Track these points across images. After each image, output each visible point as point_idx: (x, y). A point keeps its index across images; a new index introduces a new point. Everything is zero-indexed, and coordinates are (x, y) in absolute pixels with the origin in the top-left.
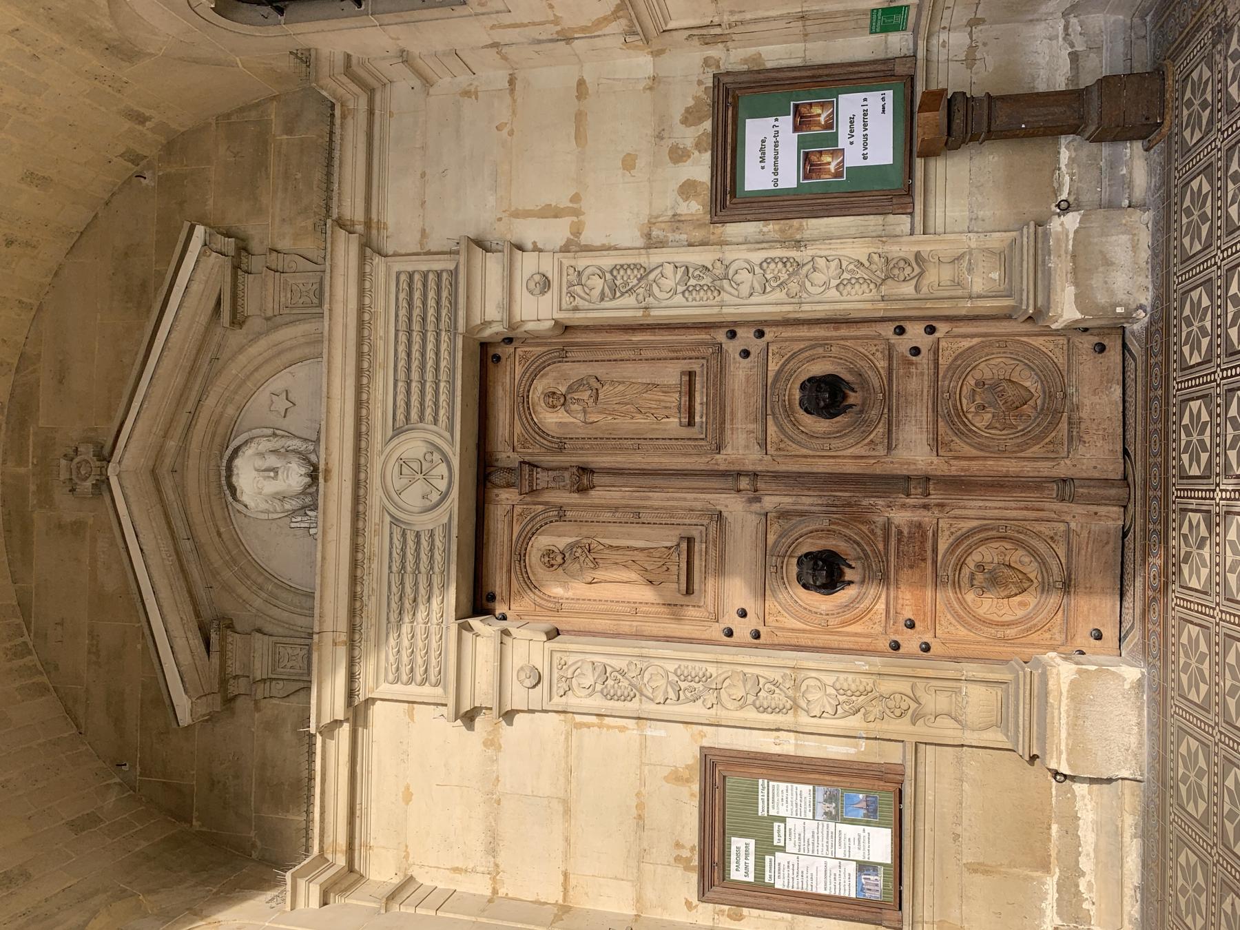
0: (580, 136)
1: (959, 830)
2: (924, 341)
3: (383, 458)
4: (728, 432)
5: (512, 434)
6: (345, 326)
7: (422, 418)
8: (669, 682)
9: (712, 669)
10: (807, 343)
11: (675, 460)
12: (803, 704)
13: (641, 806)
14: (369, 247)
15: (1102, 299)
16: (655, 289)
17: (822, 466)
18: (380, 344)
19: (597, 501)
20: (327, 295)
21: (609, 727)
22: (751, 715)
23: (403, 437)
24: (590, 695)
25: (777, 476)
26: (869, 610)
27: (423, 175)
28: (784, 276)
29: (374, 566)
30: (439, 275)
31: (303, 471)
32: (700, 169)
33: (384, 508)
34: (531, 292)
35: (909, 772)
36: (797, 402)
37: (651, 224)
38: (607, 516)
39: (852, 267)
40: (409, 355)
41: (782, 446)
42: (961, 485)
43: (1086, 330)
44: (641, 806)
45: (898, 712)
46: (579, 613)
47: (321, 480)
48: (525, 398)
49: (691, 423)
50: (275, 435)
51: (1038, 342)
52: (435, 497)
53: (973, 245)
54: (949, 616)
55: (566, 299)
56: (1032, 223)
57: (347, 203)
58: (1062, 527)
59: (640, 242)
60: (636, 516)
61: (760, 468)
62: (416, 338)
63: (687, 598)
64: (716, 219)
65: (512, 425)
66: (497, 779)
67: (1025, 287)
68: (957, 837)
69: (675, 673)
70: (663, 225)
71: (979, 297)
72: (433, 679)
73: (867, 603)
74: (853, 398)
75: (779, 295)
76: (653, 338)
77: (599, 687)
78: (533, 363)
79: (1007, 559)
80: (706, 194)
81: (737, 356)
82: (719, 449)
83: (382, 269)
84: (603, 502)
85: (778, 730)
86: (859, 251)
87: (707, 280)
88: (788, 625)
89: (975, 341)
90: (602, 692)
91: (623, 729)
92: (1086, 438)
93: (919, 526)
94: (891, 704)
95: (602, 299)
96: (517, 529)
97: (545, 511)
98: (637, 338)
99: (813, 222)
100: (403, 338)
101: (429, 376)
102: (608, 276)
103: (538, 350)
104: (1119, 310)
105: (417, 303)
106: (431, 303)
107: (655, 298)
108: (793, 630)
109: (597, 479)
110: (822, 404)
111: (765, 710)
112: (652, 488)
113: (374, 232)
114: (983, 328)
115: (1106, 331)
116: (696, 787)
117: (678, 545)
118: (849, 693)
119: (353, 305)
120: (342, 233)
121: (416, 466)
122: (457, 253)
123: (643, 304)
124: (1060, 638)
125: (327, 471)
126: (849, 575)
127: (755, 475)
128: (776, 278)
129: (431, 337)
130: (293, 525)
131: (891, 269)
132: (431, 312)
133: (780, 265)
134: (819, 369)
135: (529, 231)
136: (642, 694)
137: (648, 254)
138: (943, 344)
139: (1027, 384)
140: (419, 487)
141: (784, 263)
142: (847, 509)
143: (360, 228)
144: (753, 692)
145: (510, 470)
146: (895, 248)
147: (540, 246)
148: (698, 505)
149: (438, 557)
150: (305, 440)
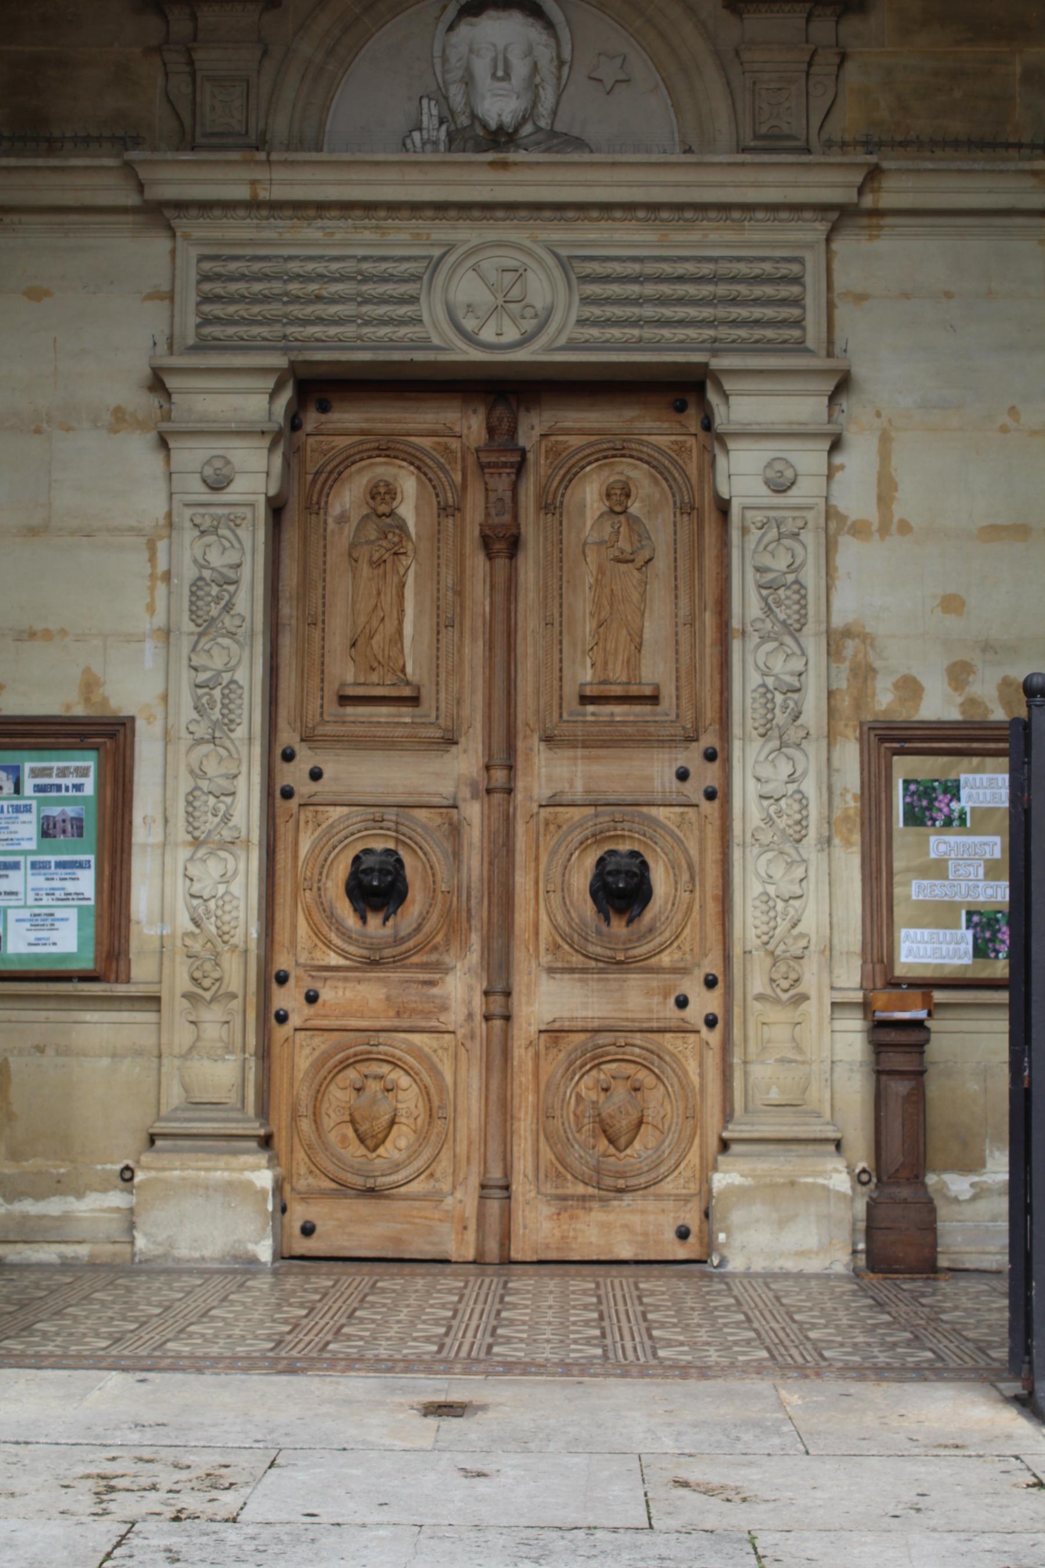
0: (993, 532)
1: (50, 1051)
2: (695, 1013)
3: (527, 243)
4: (570, 753)
5: (568, 432)
6: (721, 185)
7: (586, 301)
8: (219, 673)
9: (240, 732)
10: (696, 858)
11: (530, 678)
12: (200, 853)
13: (47, 635)
15: (737, 1216)
16: (770, 646)
17: (523, 882)
18: (695, 236)
19: (468, 563)
20: (766, 158)
21: (152, 589)
22: (185, 784)
23: (557, 273)
24: (195, 561)
25: (509, 820)
26: (328, 944)
27: (948, 295)
28: (782, 823)
29: (367, 235)
30: (798, 323)
31: (507, 119)
32: (938, 705)
33: (451, 247)
34: (769, 465)
35: (121, 989)
36: (613, 847)
37: (866, 638)
38: (448, 577)
39: (792, 912)
40: (681, 279)
41: (552, 828)
42: (499, 1057)
43: (707, 1215)
44: (47, 635)
45: (198, 974)
46: (305, 539)
47: (490, 156)
48: (621, 452)
49: (585, 700)
50: (561, 63)
51: (693, 1157)
52: (469, 324)
53: (814, 1067)
54: (323, 1047)
55: (759, 516)
56: (838, 1135)
57: (908, 182)
58: (446, 1187)
59: (837, 622)
60: (446, 621)
61: (520, 796)
62: (706, 290)
63: (335, 699)
64: (865, 728)
65: (581, 432)
66: (69, 429)
67: (756, 1127)
68: (41, 1050)
69: (232, 681)
70: (860, 656)
71: (746, 1074)
72: (207, 330)
73: (337, 941)
74: (618, 927)
75: (755, 816)
76: (708, 641)
77: (207, 574)
78: (674, 462)
79: (403, 1120)
80: (902, 715)
81: (679, 764)
82: (548, 739)
83: (810, 237)
84: (468, 572)
85: (166, 821)
86: (813, 921)
87: (780, 718)
88: (302, 835)
89: (695, 1079)
90: (201, 578)
91: (151, 609)
92: (565, 1216)
93: (444, 1008)
94: (208, 966)
95: (758, 569)
96: (426, 442)
97: (452, 484)
98: (709, 619)
99: (856, 860)
100: (706, 269)
101: (649, 311)
102: (790, 578)
103: (692, 470)
104: (722, 1237)
105: (758, 291)
106: (758, 312)
107: (758, 646)
108: (296, 844)
109: (501, 562)
110: (610, 879)
111: (189, 803)
112: (490, 646)
113: (865, 221)
114: (714, 1088)
115: (706, 1239)
116: (79, 711)
117: (408, 683)
118: (219, 913)
119: (752, 196)
120: (858, 178)
121: (516, 293)
122: (830, 354)
123: (749, 629)
124: (302, 1184)
125: (504, 165)
126: (374, 921)
127: (509, 791)
128: (779, 813)
129: (707, 312)
130: (425, 102)
131: (786, 962)
132: (743, 312)
133: (798, 817)
134: (660, 879)
135: (859, 459)
136: (200, 635)
137: (817, 634)
138: (692, 1038)
139: (637, 1145)
140: (483, 296)
141: (799, 822)
142: (464, 914)
143: (868, 201)
144: (213, 788)
145: (513, 432)
146: (814, 968)
147: (838, 476)
148: (466, 712)
149: (383, 331)
150: (554, 113)
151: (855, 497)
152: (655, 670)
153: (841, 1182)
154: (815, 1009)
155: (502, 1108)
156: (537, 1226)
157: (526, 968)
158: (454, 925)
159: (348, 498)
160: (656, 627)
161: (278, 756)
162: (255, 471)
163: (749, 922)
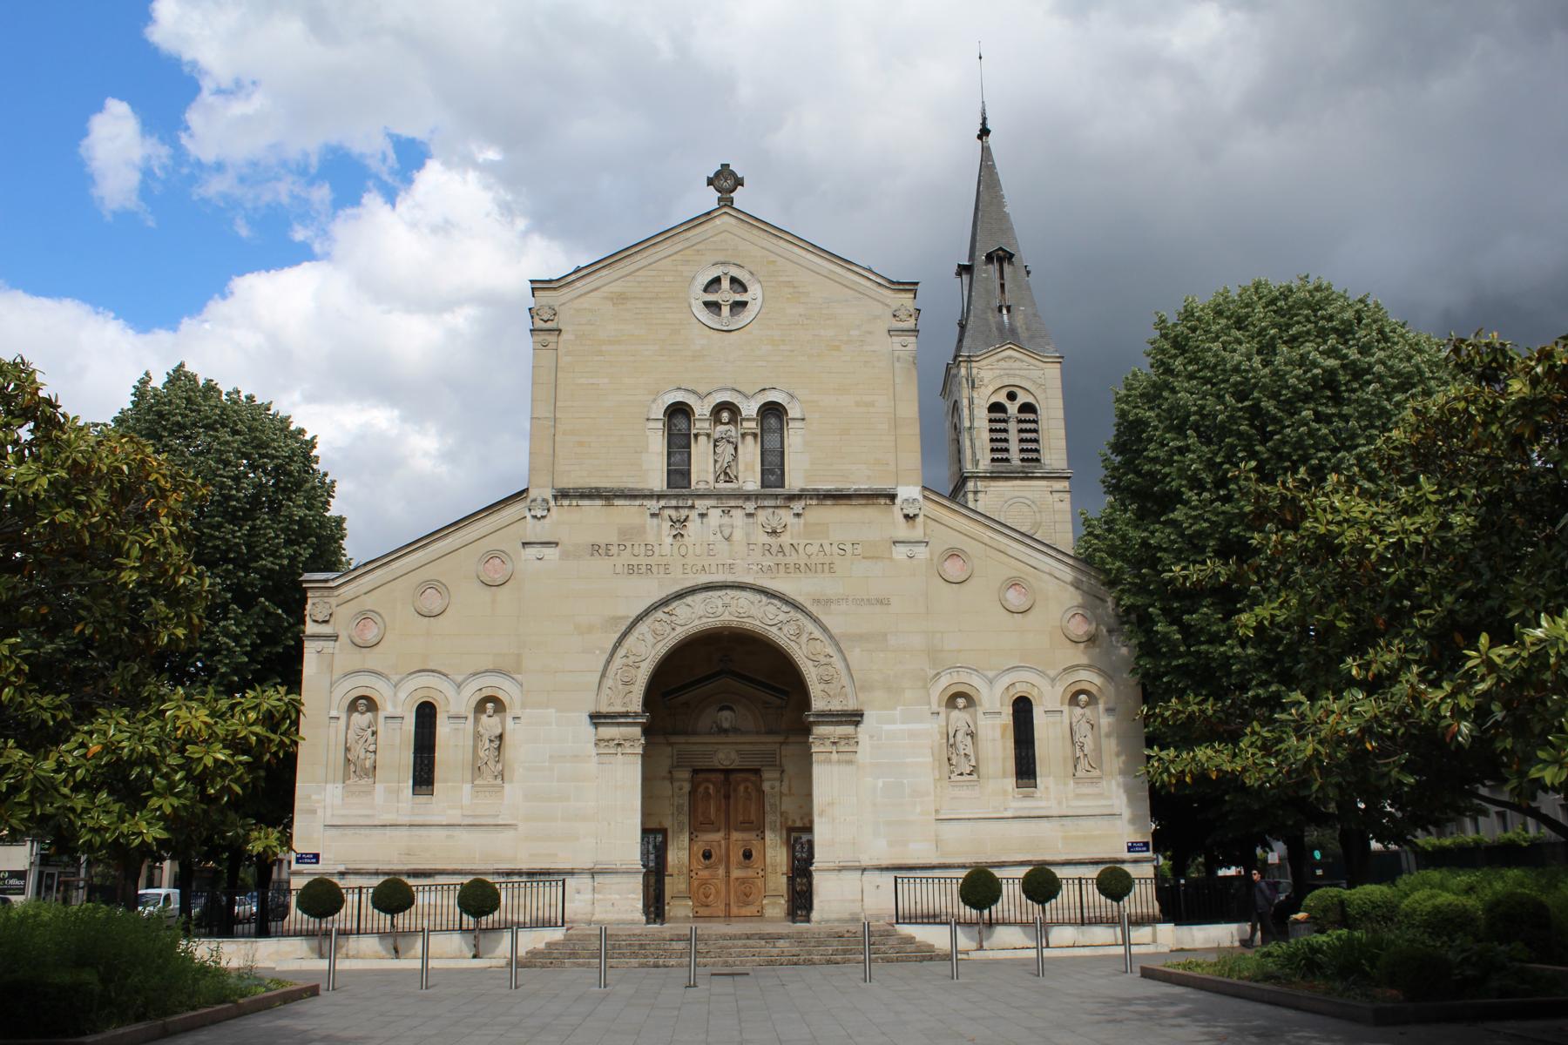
42: (728, 883)
135: (786, 783)
151: (785, 789)
152: (753, 817)
155: (728, 892)
156: (734, 910)
158: (720, 861)
159: (701, 789)
162: (687, 787)
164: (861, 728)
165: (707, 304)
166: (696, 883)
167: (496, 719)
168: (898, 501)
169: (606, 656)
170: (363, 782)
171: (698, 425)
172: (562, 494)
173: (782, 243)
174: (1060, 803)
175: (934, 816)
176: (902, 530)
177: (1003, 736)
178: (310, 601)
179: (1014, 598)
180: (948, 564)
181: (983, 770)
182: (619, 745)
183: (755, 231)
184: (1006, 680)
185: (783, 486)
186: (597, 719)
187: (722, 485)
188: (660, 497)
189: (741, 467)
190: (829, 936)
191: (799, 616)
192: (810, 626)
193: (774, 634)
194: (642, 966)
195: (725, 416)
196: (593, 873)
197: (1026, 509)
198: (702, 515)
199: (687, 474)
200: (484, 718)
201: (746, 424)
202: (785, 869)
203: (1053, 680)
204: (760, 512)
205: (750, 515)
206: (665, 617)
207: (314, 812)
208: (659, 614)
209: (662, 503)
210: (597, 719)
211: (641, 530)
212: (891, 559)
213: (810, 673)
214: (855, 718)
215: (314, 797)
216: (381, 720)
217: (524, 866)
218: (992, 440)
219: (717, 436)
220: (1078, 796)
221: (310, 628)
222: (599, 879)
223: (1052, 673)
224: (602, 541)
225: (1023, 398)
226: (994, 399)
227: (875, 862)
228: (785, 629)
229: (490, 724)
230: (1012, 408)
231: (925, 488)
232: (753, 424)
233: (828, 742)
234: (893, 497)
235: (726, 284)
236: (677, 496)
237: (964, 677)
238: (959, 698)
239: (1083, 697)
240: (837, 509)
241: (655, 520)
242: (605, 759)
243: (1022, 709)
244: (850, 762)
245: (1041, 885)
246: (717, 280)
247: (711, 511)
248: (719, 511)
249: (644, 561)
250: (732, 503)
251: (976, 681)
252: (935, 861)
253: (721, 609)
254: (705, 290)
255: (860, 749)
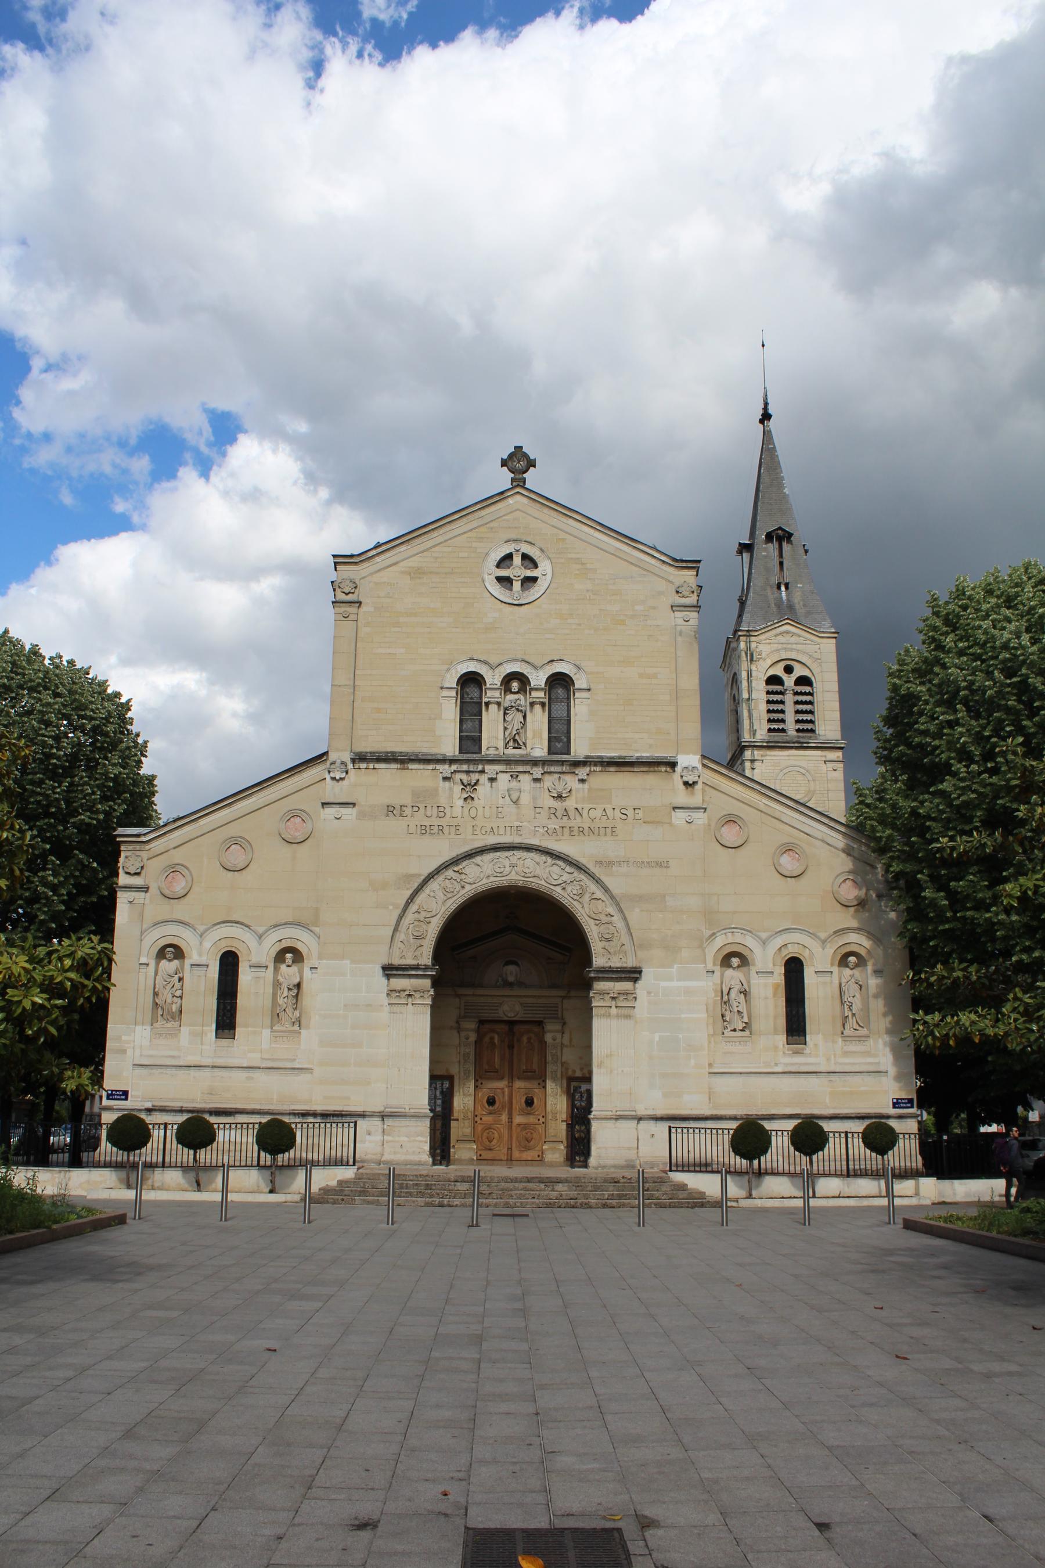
14: (564, 998)
17: (514, 1101)
42: (510, 1128)
134: (535, 1100)
135: (566, 1036)
151: (566, 1041)
152: (535, 1067)
153: (562, 1147)
154: (559, 1121)
155: (511, 1137)
156: (516, 1154)
157: (515, 1113)
158: (503, 1107)
159: (487, 1039)
160: (535, 1059)
161: (476, 1081)
162: (473, 1037)
163: (549, 1108)
164: (640, 984)
165: (499, 579)
166: (480, 1128)
167: (294, 969)
168: (678, 769)
169: (399, 911)
170: (169, 1025)
171: (489, 694)
172: (360, 758)
173: (571, 522)
174: (828, 1060)
175: (707, 1070)
176: (682, 797)
177: (775, 994)
178: (123, 855)
179: (787, 863)
180: (725, 830)
181: (755, 1026)
182: (410, 995)
183: (546, 510)
184: (779, 941)
185: (568, 753)
186: (390, 970)
187: (511, 751)
188: (452, 761)
189: (529, 734)
190: (605, 1181)
191: (582, 877)
192: (592, 887)
193: (558, 893)
194: (427, 1204)
195: (515, 685)
196: (383, 1116)
197: (800, 778)
198: (492, 780)
199: (478, 740)
200: (283, 967)
201: (534, 694)
202: (564, 1116)
203: (824, 942)
204: (547, 777)
205: (537, 780)
206: (455, 875)
207: (124, 1052)
208: (450, 873)
209: (454, 767)
210: (390, 970)
211: (434, 792)
212: (670, 824)
213: (592, 931)
214: (633, 974)
215: (124, 1038)
216: (187, 966)
217: (319, 1108)
218: (769, 711)
219: (506, 705)
220: (846, 1054)
221: (123, 879)
222: (389, 1122)
223: (823, 935)
224: (396, 802)
225: (799, 671)
226: (771, 672)
227: (650, 1112)
228: (569, 889)
229: (289, 973)
230: (789, 681)
231: (703, 757)
232: (541, 694)
233: (607, 997)
234: (673, 765)
235: (517, 560)
236: (468, 761)
237: (738, 938)
238: (734, 958)
239: (852, 959)
240: (620, 775)
241: (447, 783)
242: (396, 1009)
243: (794, 969)
244: (628, 1017)
245: (809, 1137)
246: (509, 557)
247: (501, 776)
248: (507, 776)
249: (436, 822)
250: (520, 768)
251: (750, 941)
252: (707, 1112)
253: (508, 869)
254: (498, 566)
255: (637, 1004)
